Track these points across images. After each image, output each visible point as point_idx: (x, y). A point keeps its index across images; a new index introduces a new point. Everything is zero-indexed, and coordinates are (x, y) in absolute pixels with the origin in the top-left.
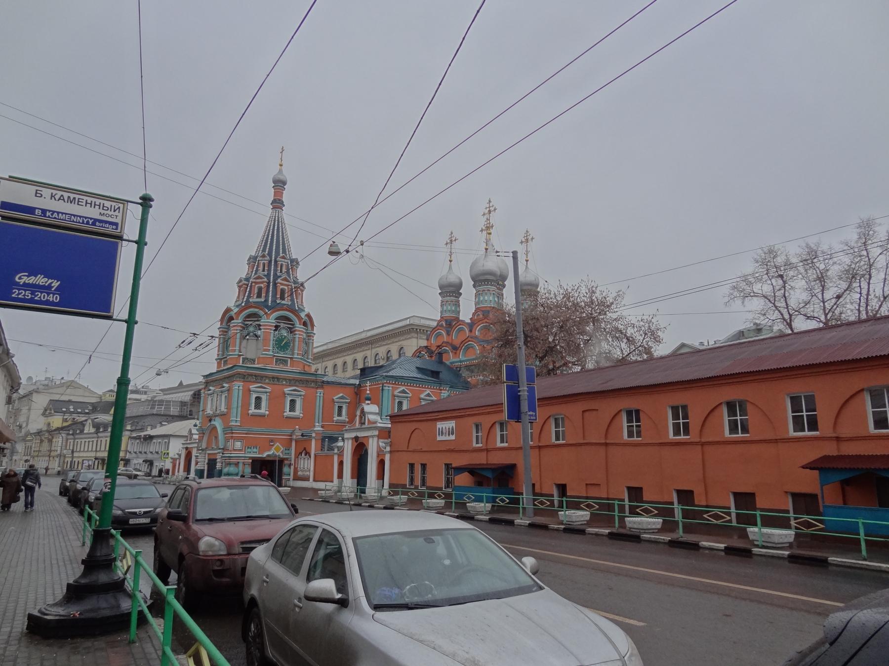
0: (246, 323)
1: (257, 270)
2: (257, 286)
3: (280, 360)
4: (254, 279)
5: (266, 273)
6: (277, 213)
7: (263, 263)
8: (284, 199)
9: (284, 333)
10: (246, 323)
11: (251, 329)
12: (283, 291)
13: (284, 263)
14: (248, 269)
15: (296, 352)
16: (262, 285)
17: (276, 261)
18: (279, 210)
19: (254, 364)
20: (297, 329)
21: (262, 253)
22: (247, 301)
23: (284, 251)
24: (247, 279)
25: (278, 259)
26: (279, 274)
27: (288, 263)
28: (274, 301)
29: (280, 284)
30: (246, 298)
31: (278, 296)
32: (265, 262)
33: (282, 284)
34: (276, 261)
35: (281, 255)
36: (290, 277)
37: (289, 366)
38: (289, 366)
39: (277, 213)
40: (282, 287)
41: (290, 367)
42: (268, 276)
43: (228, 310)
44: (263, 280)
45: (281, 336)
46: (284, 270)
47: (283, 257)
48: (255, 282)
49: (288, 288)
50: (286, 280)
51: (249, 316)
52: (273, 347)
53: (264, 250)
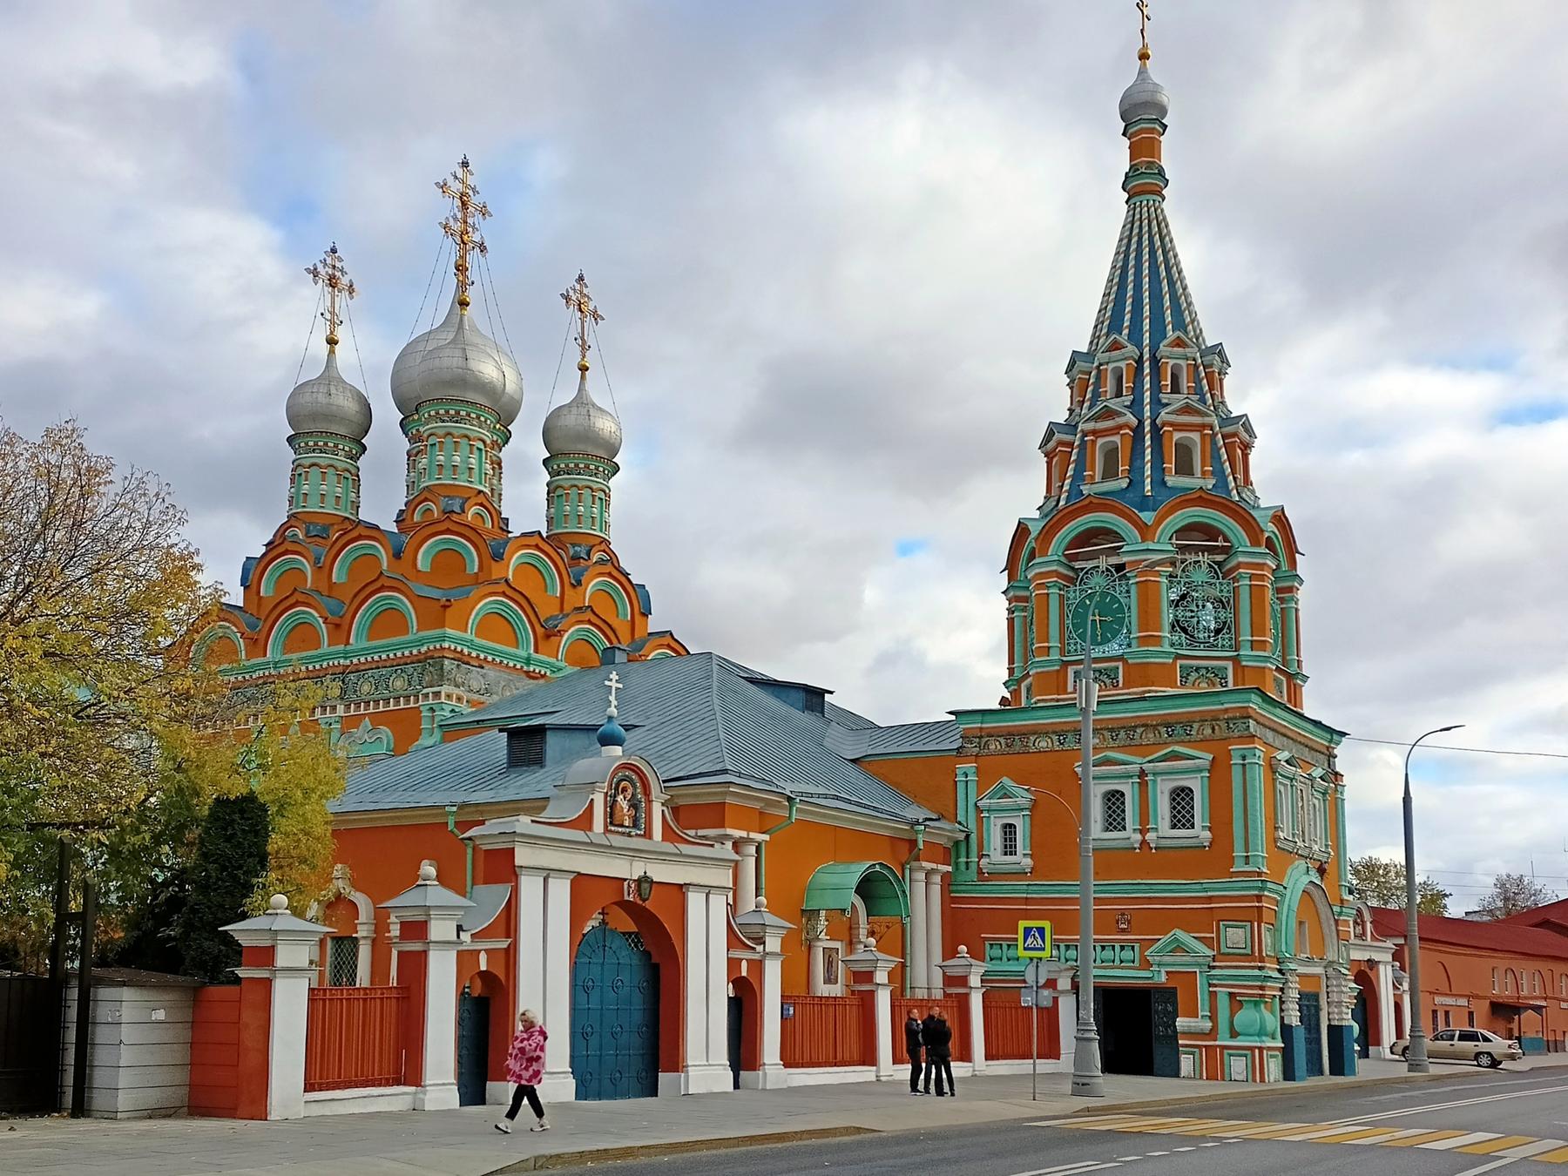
0: (1077, 565)
1: (1096, 396)
2: (1100, 441)
3: (1197, 669)
4: (1095, 418)
5: (1127, 400)
7: (1113, 369)
8: (1166, 162)
10: (1077, 565)
11: (1097, 581)
12: (1184, 451)
14: (1071, 397)
15: (1246, 637)
16: (1117, 439)
17: (1155, 360)
18: (1148, 197)
19: (1116, 687)
20: (1241, 559)
21: (1108, 335)
22: (1075, 492)
23: (1180, 324)
24: (1070, 427)
26: (1164, 398)
27: (1194, 360)
28: (1160, 483)
29: (1171, 424)
30: (1068, 482)
32: (1123, 364)
33: (1179, 427)
34: (1155, 360)
35: (1171, 334)
36: (1203, 401)
40: (1177, 436)
42: (1137, 406)
43: (1022, 531)
44: (1120, 420)
46: (1184, 384)
47: (1179, 343)
48: (1094, 432)
49: (1203, 436)
50: (1187, 410)
51: (1087, 537)
53: (1115, 326)
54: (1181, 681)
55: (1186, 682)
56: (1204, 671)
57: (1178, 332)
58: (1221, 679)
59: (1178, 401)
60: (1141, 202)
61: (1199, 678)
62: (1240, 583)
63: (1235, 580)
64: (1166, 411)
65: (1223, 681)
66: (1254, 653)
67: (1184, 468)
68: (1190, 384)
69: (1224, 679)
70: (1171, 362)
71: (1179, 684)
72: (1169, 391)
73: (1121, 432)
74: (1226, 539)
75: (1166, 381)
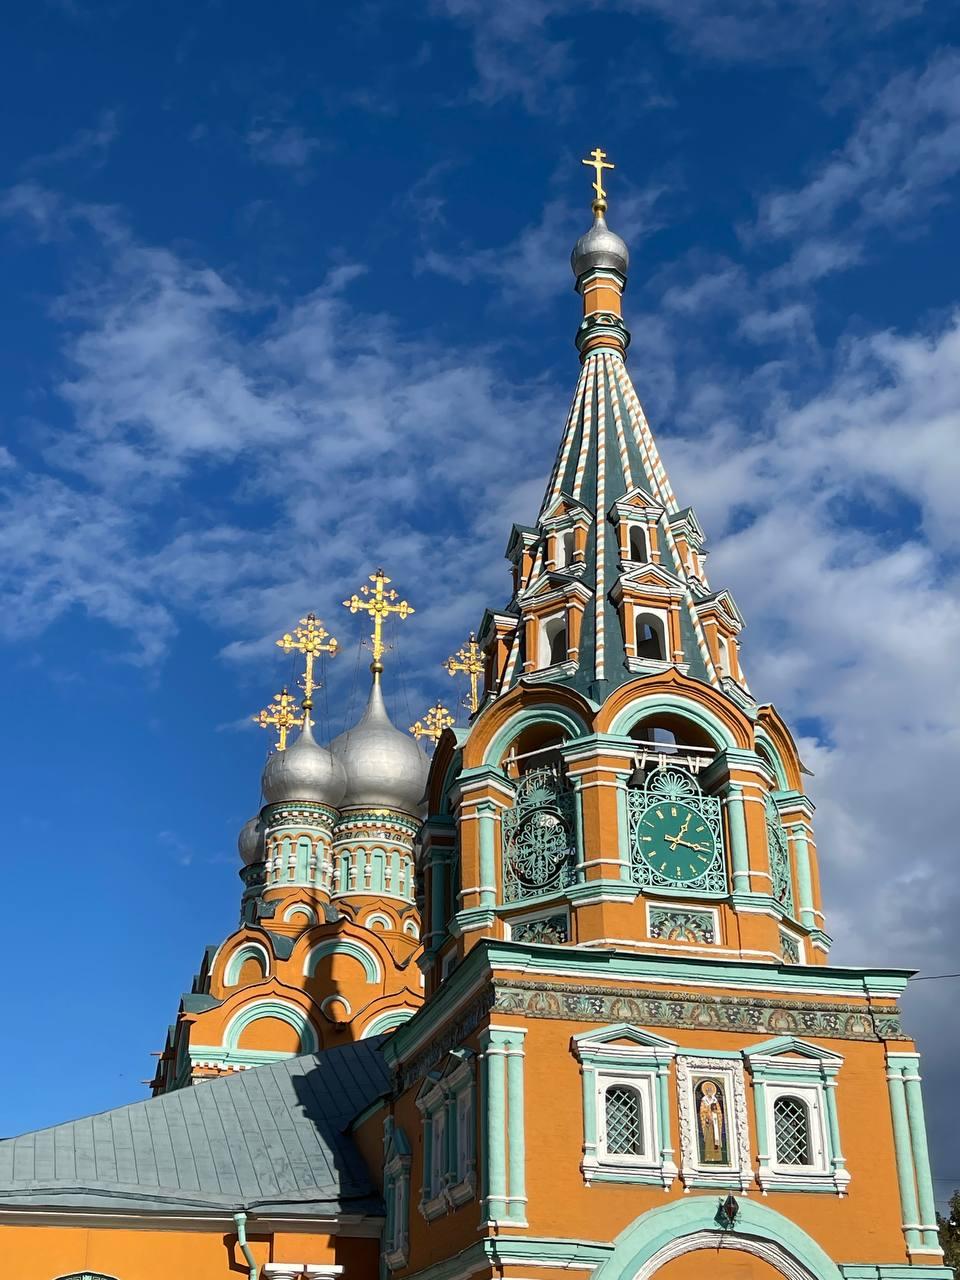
6: (601, 363)
9: (673, 789)
13: (644, 526)
15: (742, 871)
17: (612, 519)
25: (623, 508)
31: (632, 645)
35: (633, 491)
37: (718, 940)
38: (718, 940)
39: (601, 363)
41: (726, 943)
45: (666, 809)
46: (650, 550)
50: (652, 579)
52: (635, 861)
54: (653, 932)
55: (659, 934)
56: (681, 920)
57: (638, 490)
58: (705, 932)
59: (641, 569)
60: (596, 355)
61: (673, 930)
62: (730, 798)
63: (724, 795)
64: (627, 577)
65: (708, 935)
66: (754, 894)
67: (651, 647)
68: (654, 552)
69: (710, 932)
70: (631, 524)
71: (649, 935)
72: (629, 558)
73: (568, 605)
74: (706, 739)
75: (626, 546)
